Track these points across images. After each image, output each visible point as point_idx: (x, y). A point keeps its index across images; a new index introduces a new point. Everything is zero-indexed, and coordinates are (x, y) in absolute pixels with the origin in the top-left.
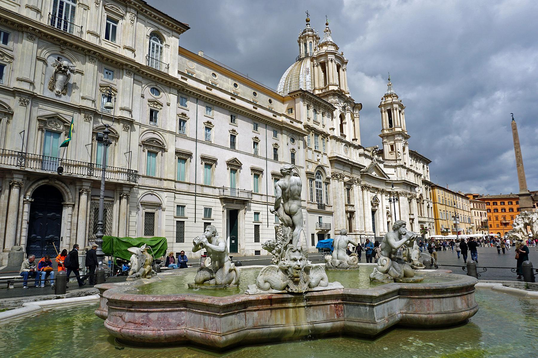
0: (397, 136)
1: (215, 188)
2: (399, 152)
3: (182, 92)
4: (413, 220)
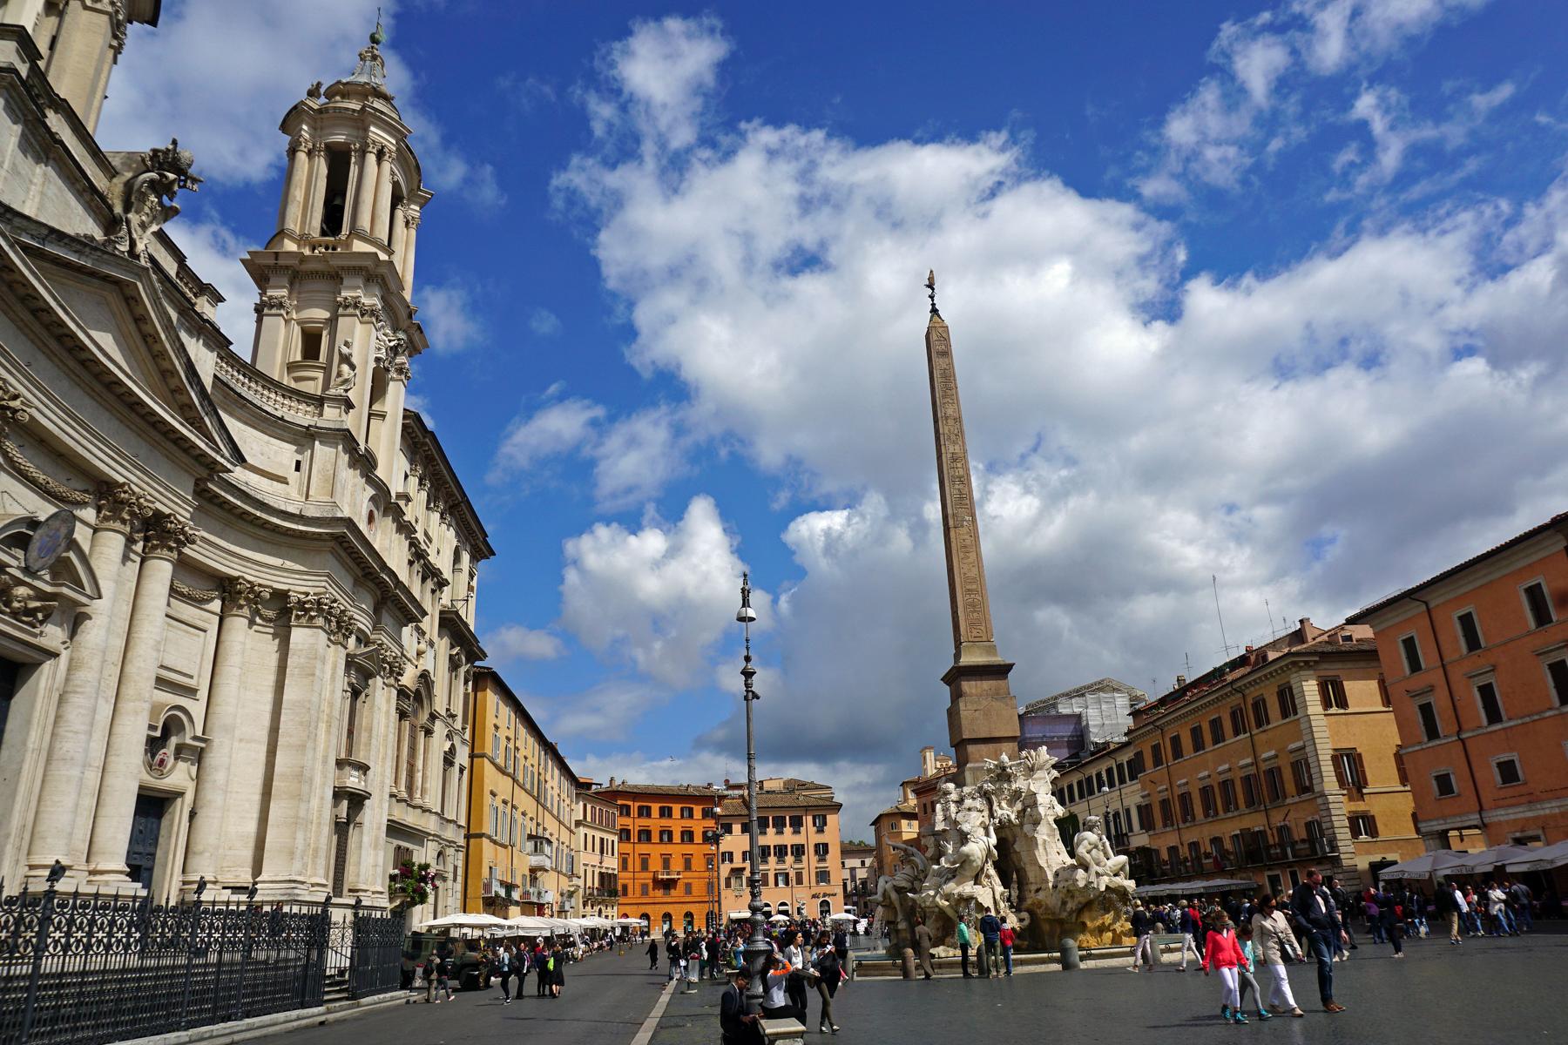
2: (346, 359)
4: (356, 800)
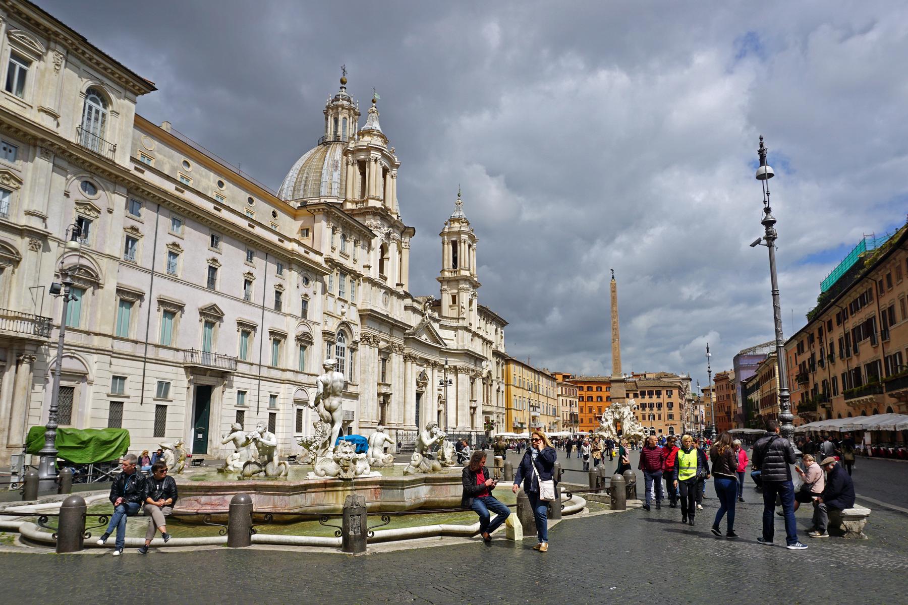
0: (463, 282)
1: (178, 350)
2: (462, 307)
3: (135, 192)
